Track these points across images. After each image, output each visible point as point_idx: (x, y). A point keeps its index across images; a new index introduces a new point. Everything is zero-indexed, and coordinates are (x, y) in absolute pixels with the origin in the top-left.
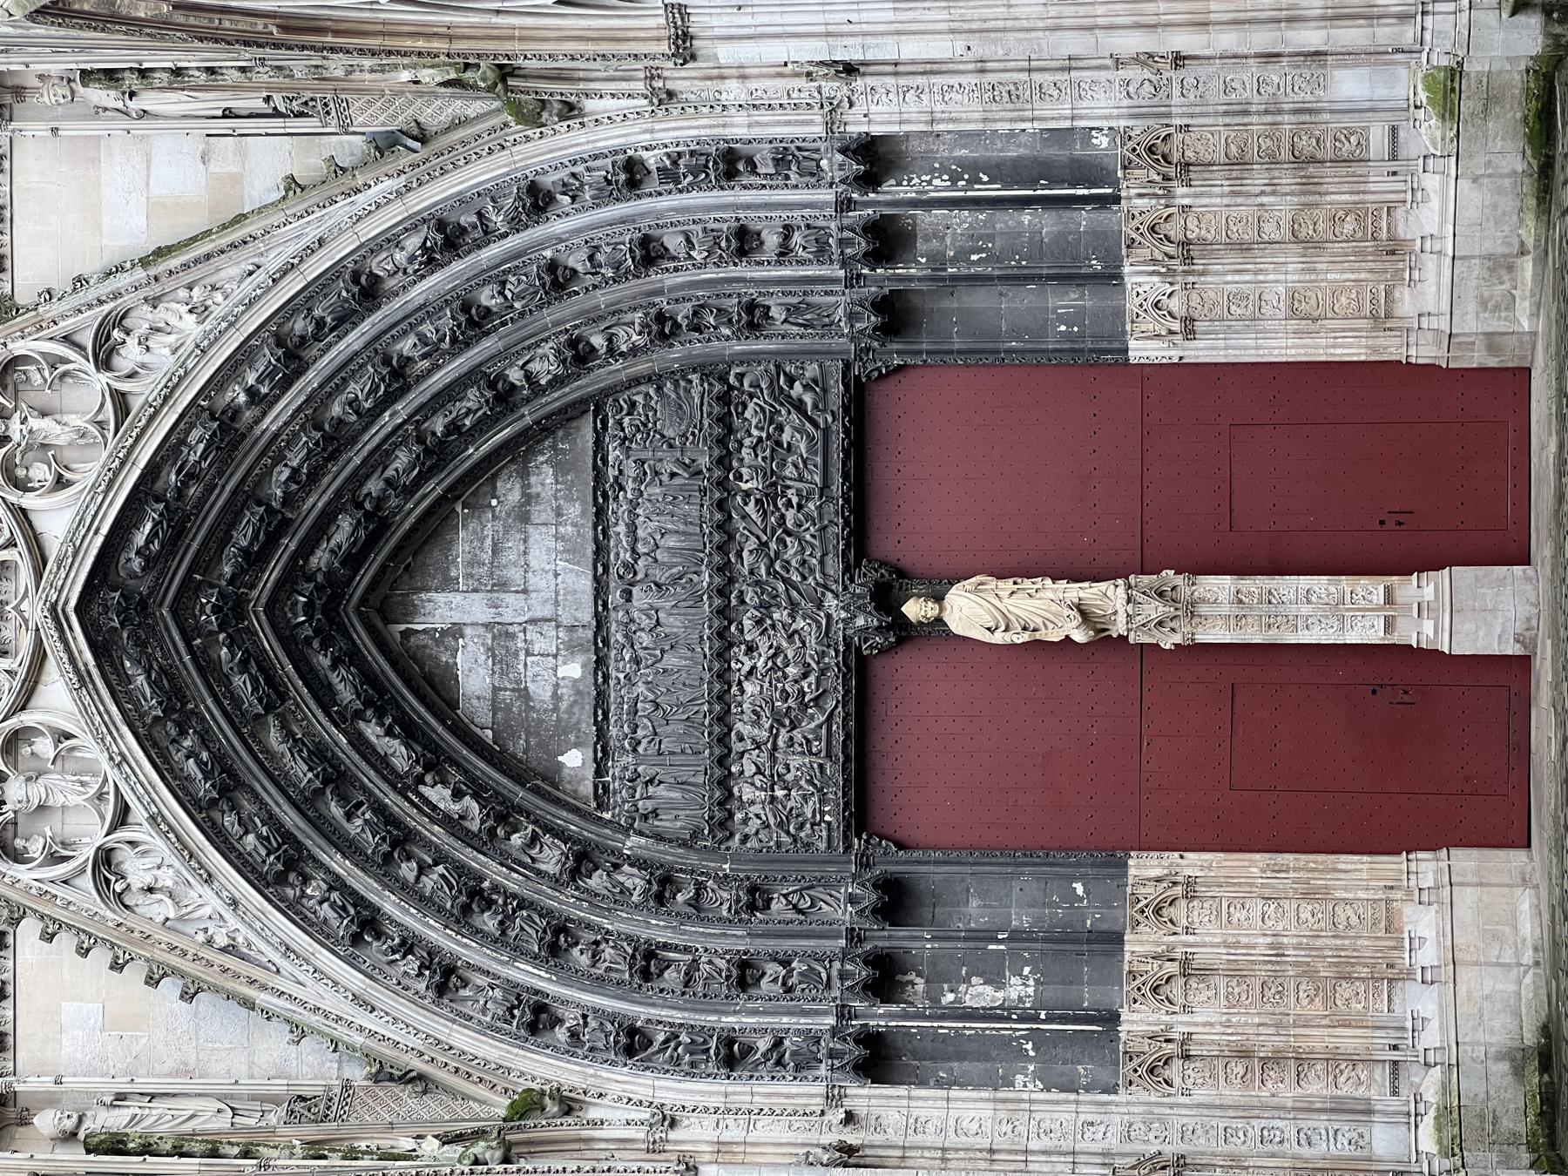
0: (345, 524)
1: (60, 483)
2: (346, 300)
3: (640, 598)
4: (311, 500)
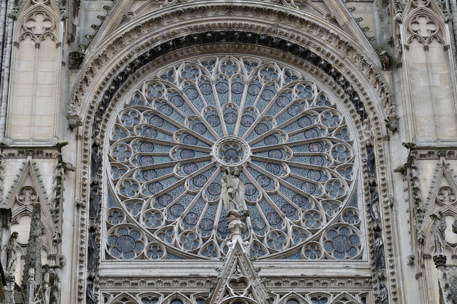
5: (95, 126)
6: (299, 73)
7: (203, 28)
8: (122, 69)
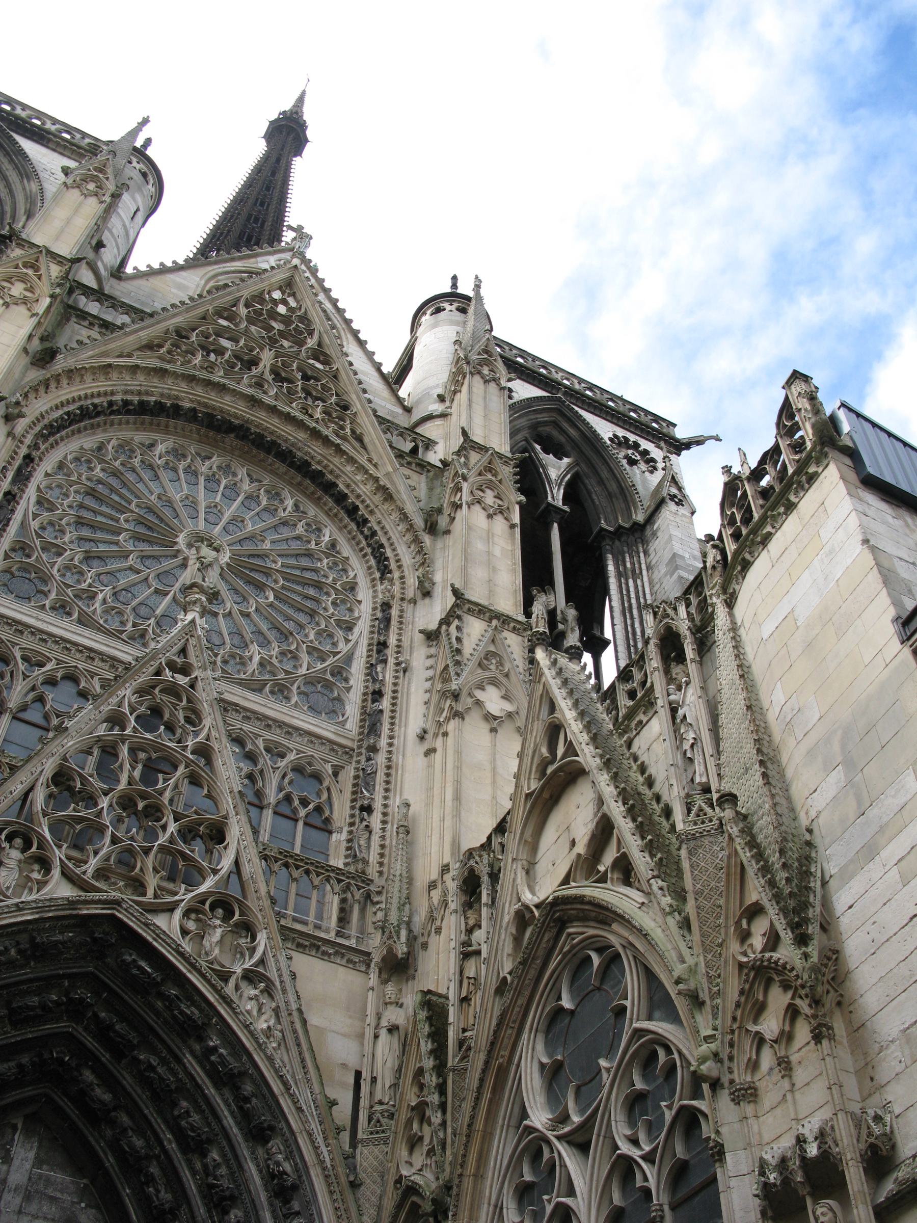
0: (107, 1097)
1: (184, 932)
2: (259, 1118)
4: (129, 1078)
5: (40, 435)
6: (312, 511)
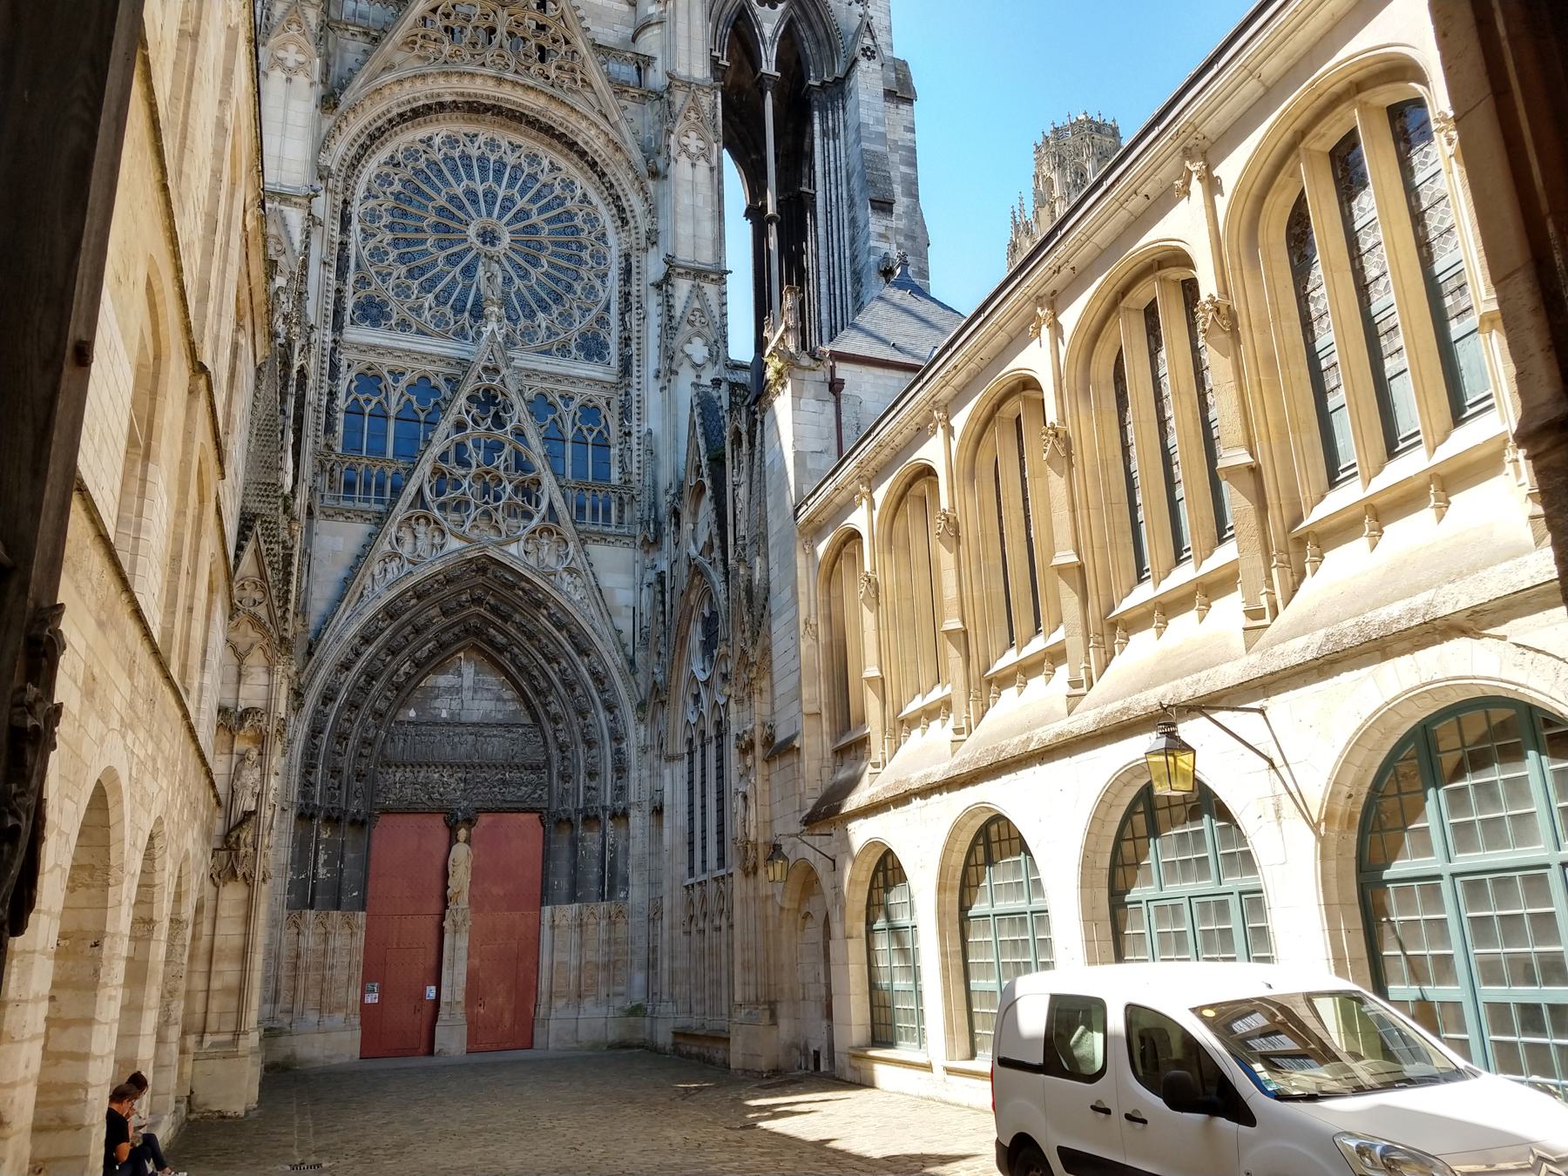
3: (471, 738)
6: (562, 162)
7: (469, 95)
8: (380, 123)
